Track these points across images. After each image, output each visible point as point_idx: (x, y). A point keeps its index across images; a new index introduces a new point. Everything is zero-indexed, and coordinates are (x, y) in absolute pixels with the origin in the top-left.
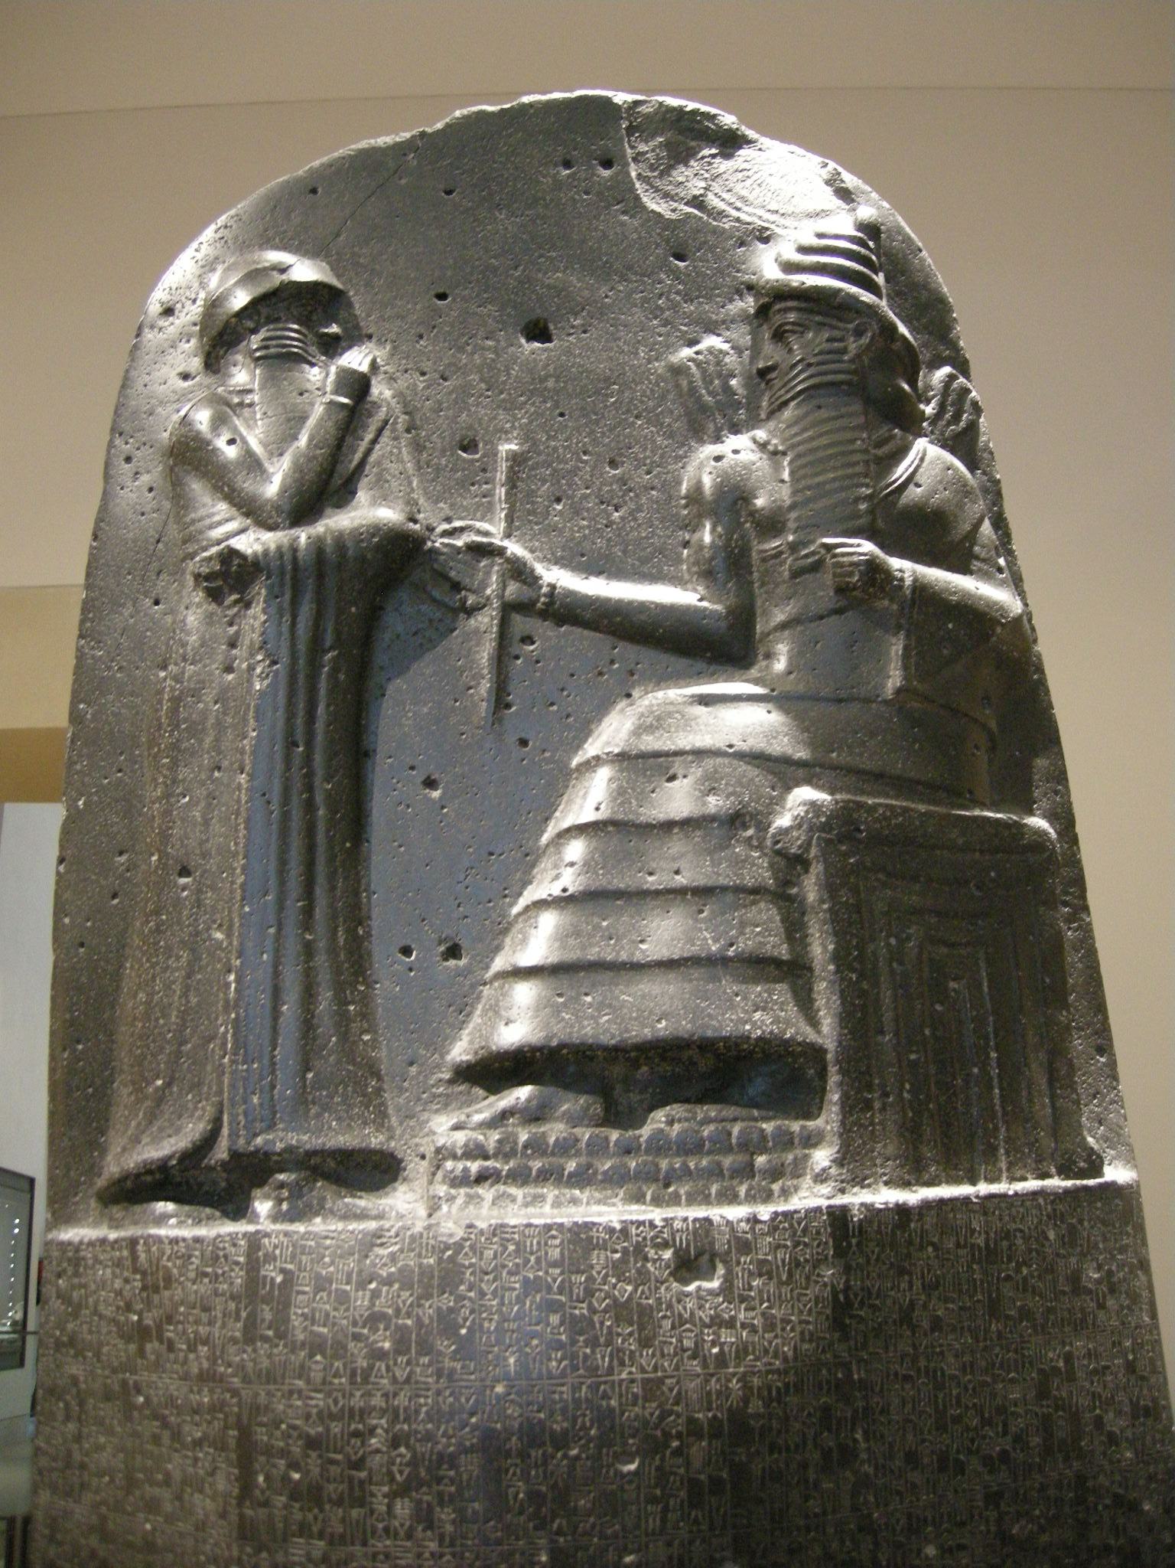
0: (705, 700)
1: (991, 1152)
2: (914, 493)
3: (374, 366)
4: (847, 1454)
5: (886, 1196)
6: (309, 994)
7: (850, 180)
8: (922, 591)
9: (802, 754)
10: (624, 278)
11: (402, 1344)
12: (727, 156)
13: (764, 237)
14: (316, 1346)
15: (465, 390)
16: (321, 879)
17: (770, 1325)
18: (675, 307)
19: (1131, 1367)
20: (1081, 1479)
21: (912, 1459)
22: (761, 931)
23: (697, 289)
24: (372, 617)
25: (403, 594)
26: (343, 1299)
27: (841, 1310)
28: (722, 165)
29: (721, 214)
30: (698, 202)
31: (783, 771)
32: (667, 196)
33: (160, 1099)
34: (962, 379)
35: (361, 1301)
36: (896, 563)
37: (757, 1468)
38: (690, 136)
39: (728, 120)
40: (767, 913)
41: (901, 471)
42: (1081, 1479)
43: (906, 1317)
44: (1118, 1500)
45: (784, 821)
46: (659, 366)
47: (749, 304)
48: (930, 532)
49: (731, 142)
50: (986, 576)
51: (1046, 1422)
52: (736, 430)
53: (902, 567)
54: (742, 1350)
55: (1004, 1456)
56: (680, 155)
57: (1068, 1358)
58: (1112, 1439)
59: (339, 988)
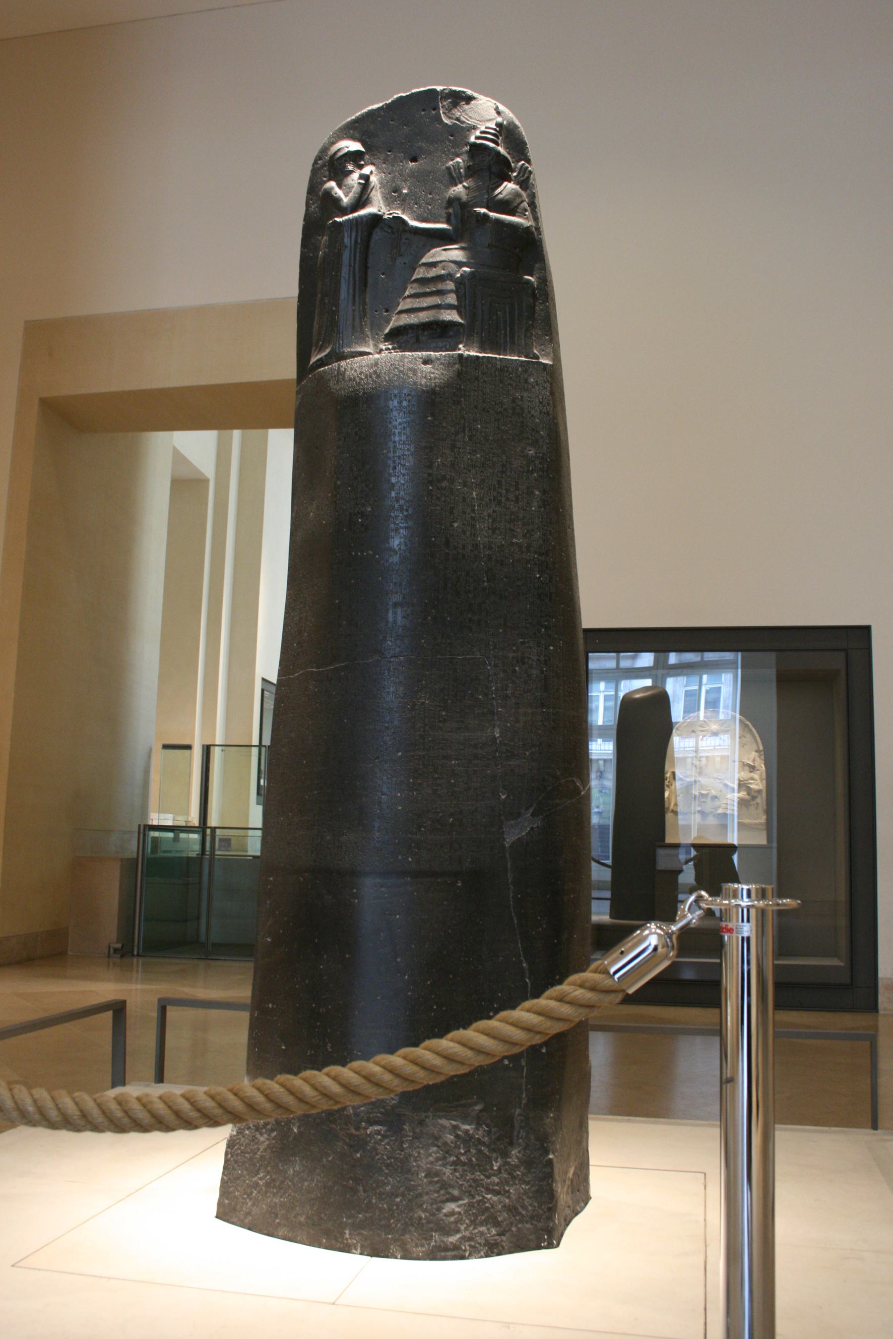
0: (445, 250)
1: (505, 350)
2: (501, 196)
3: (371, 172)
4: (459, 403)
5: (473, 353)
6: (354, 320)
7: (502, 108)
8: (498, 221)
9: (464, 260)
10: (436, 143)
11: (366, 377)
12: (468, 103)
13: (475, 128)
14: (350, 380)
15: (394, 177)
16: (357, 295)
17: (442, 374)
18: (449, 150)
19: (541, 403)
20: (522, 422)
21: (476, 407)
22: (452, 299)
23: (455, 145)
24: (370, 235)
25: (377, 230)
26: (356, 371)
27: (459, 374)
28: (466, 107)
29: (463, 122)
30: (458, 119)
31: (460, 264)
32: (450, 118)
33: (322, 346)
34: (527, 165)
35: (359, 371)
36: (491, 214)
37: (437, 400)
38: (459, 99)
39: (469, 92)
40: (454, 296)
41: (497, 192)
42: (522, 422)
43: (477, 378)
44: (533, 429)
45: (458, 275)
46: (443, 167)
47: (467, 148)
48: (507, 206)
49: (469, 99)
50: (519, 217)
51: (514, 408)
52: (461, 183)
53: (493, 215)
54: (435, 378)
55: (501, 412)
56: (455, 105)
57: (522, 397)
58: (533, 416)
59: (360, 318)
